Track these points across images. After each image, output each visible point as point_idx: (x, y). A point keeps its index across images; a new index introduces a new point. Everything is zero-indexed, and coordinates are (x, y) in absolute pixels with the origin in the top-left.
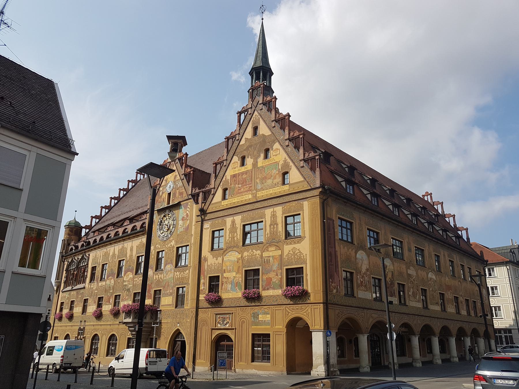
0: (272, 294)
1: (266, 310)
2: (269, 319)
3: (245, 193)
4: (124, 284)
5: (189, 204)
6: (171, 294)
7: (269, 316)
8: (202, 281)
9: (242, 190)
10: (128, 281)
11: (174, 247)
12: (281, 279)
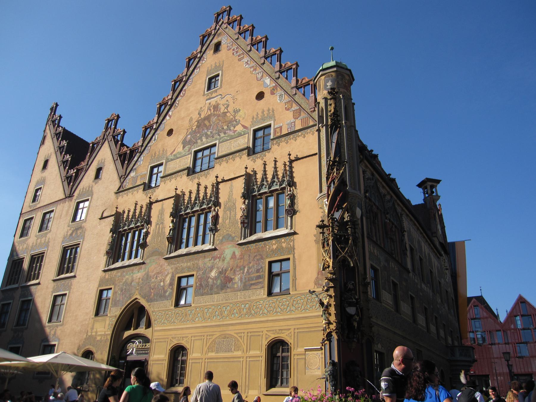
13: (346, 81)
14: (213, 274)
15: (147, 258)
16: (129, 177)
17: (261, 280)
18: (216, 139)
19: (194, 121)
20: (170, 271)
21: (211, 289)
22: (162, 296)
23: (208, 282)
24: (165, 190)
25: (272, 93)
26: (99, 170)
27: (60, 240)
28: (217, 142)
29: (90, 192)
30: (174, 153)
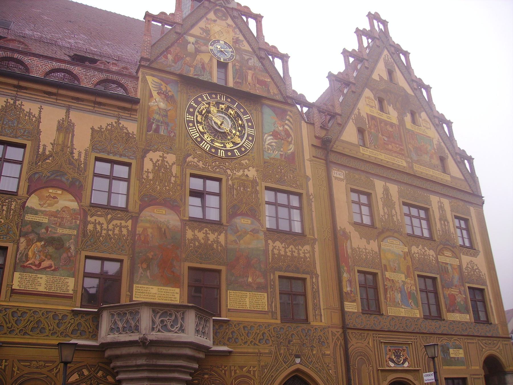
0: (458, 319)
1: (457, 343)
2: (462, 356)
3: (396, 155)
4: (29, 217)
5: (289, 113)
6: (260, 288)
7: (461, 351)
8: (345, 276)
9: (390, 147)
10: (54, 214)
11: (254, 183)
12: (466, 298)
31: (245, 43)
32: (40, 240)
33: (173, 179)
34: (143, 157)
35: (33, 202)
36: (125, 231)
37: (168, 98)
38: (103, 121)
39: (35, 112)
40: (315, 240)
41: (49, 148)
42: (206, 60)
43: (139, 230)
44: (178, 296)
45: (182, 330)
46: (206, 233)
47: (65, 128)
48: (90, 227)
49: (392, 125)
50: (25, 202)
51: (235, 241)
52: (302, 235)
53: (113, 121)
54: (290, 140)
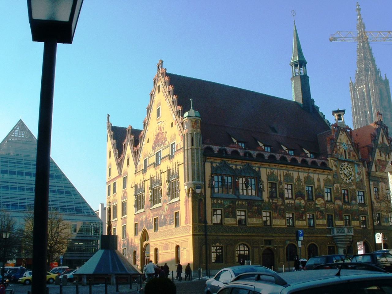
4: (317, 206)
10: (320, 205)
11: (355, 190)
13: (193, 123)
14: (162, 218)
15: (146, 208)
16: (138, 165)
17: (173, 221)
18: (161, 148)
19: (155, 135)
20: (152, 215)
21: (162, 224)
22: (150, 228)
23: (161, 221)
24: (147, 176)
25: (175, 125)
26: (128, 160)
27: (120, 198)
28: (161, 149)
29: (126, 173)
30: (150, 153)
31: (349, 142)
32: (319, 211)
33: (339, 192)
34: (333, 186)
35: (317, 202)
36: (333, 208)
37: (336, 167)
38: (325, 177)
39: (313, 177)
40: (367, 205)
41: (317, 186)
42: (342, 151)
43: (335, 207)
44: (343, 223)
45: (352, 232)
46: (347, 206)
47: (319, 180)
48: (327, 207)
49: (383, 161)
50: (315, 202)
51: (352, 208)
52: (364, 204)
53: (326, 176)
54: (361, 174)
